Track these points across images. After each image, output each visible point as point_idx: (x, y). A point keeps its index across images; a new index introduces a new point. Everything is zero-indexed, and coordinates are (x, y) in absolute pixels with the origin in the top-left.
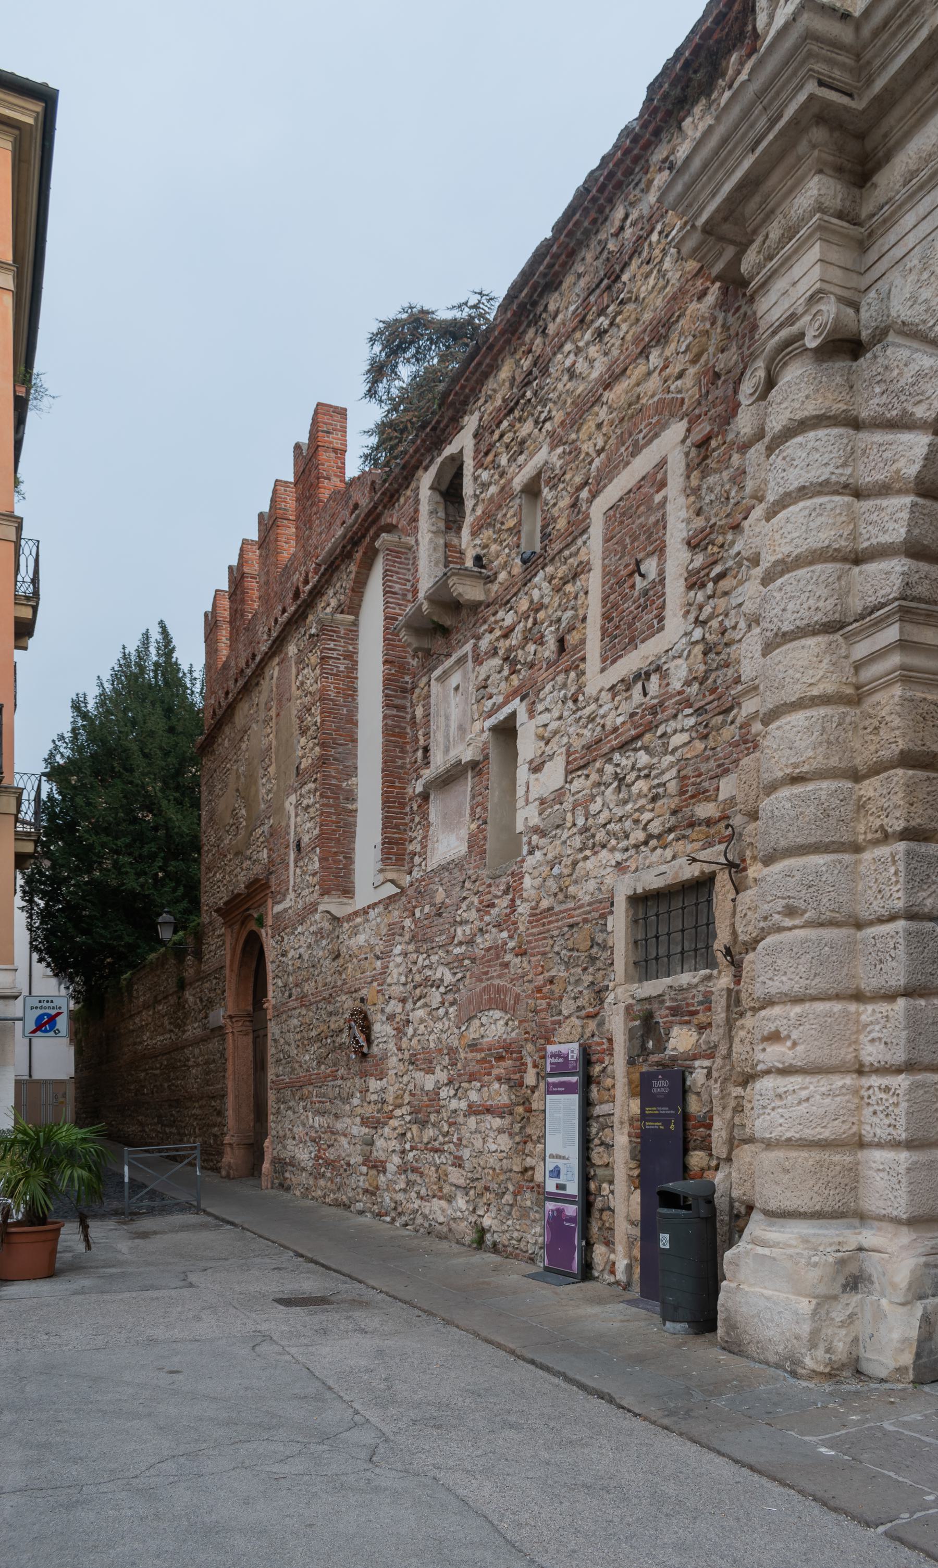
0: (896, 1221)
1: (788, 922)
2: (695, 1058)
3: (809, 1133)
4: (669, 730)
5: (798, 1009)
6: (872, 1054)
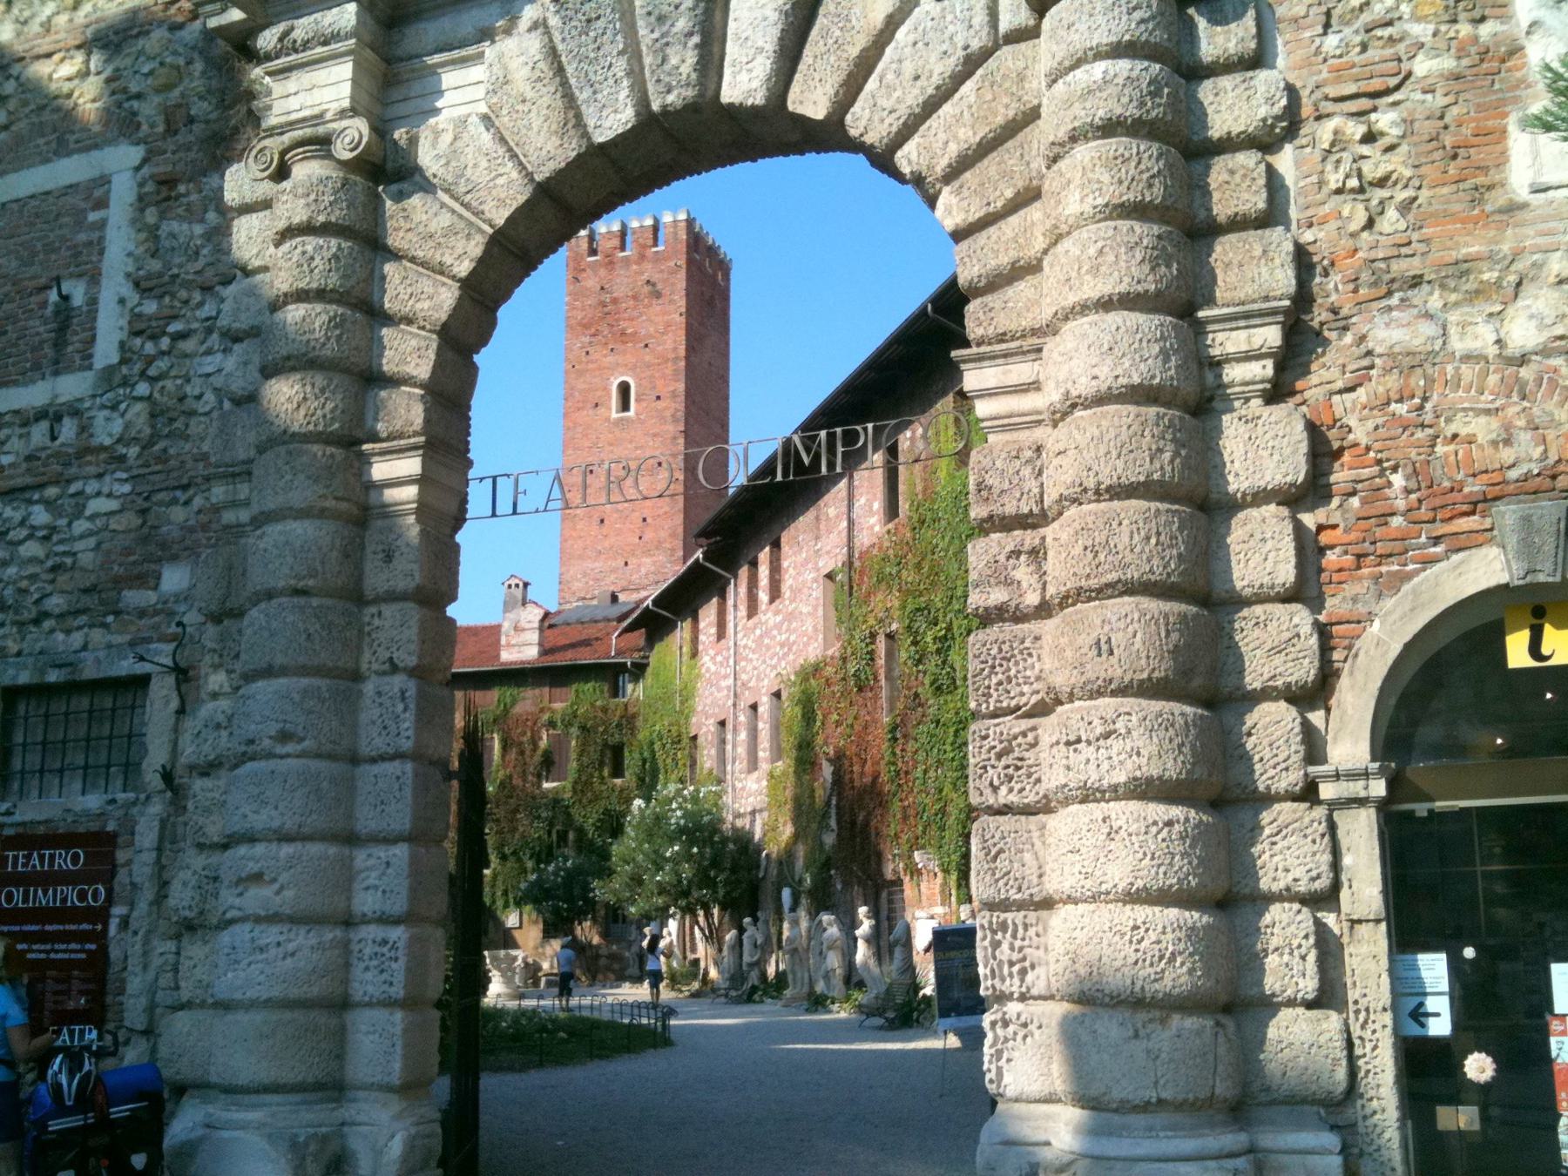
0: (389, 1089)
3: (295, 993)
4: (89, 490)
5: (287, 850)
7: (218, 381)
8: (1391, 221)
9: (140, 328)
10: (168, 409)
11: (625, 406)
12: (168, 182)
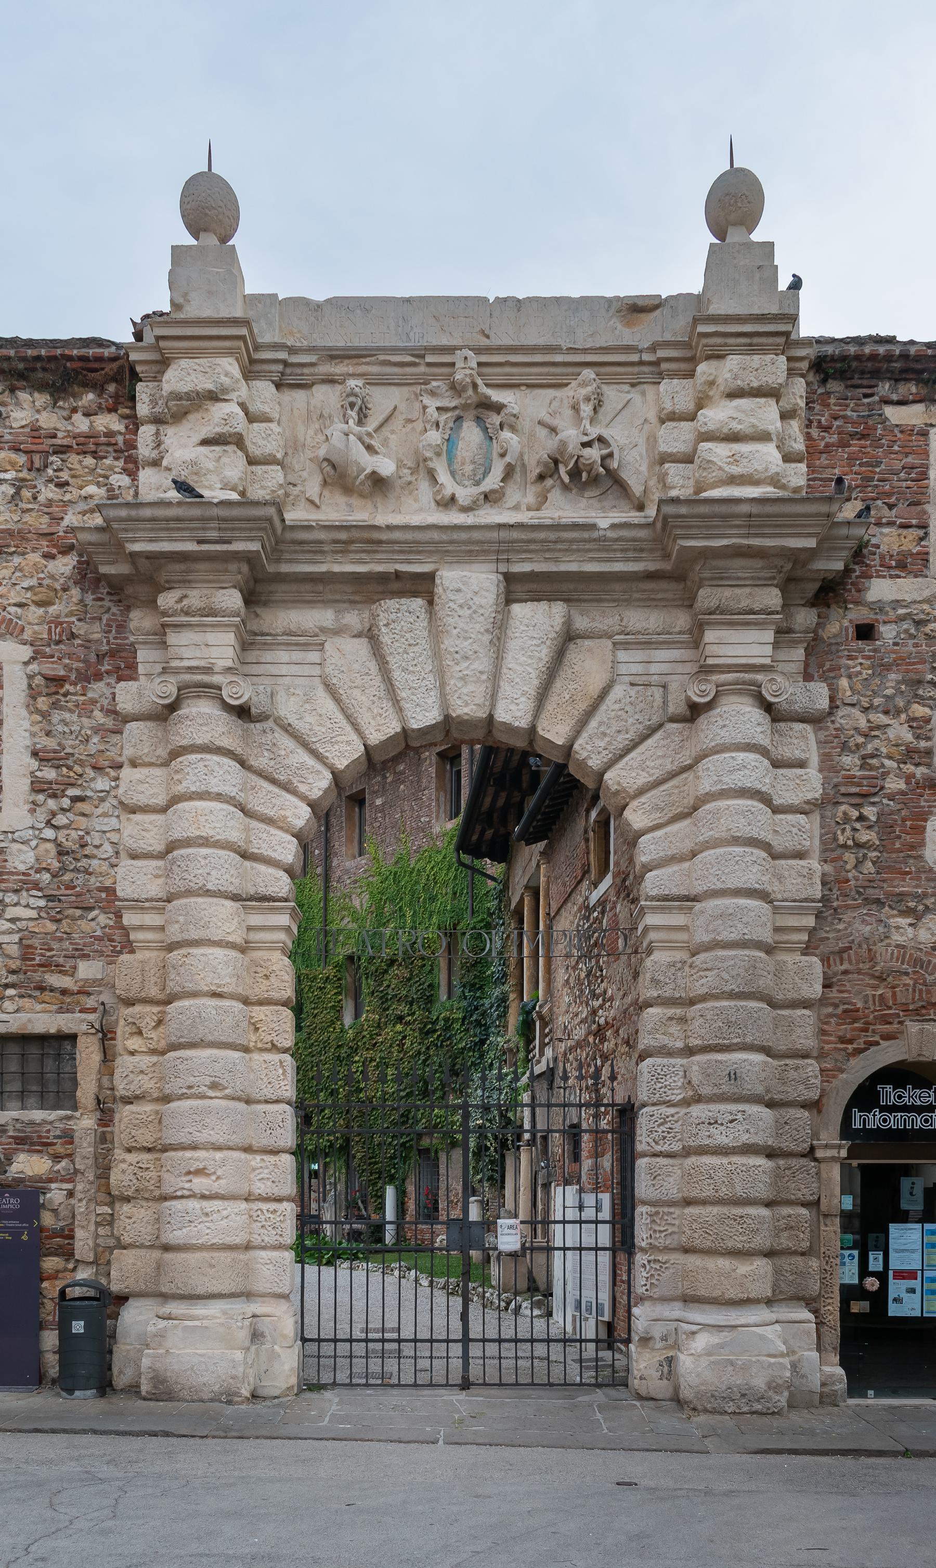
1: (211, 1093)
2: (50, 1180)
3: (229, 1240)
6: (260, 1188)
7: (114, 837)
8: (869, 867)
9: (38, 786)
10: (73, 852)
12: (56, 681)
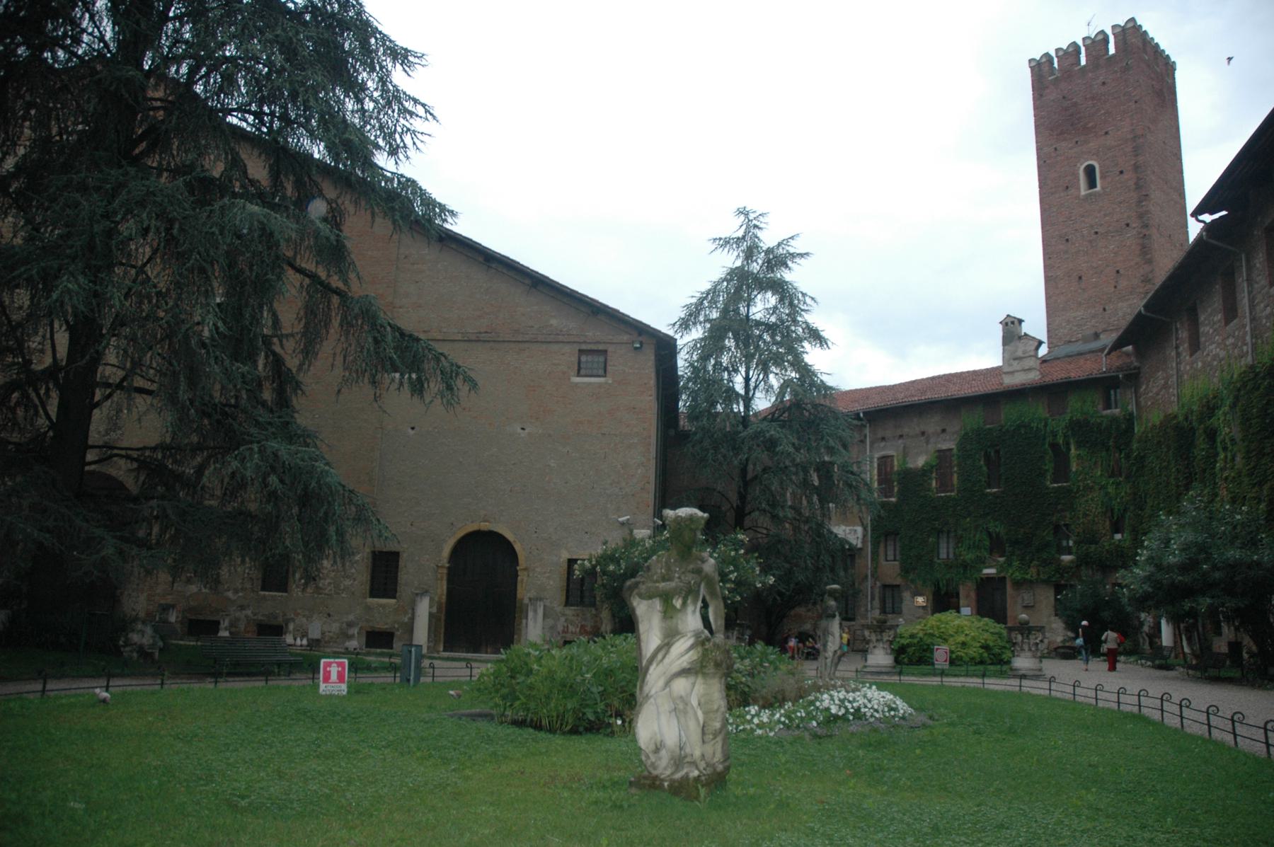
11: (1092, 183)
